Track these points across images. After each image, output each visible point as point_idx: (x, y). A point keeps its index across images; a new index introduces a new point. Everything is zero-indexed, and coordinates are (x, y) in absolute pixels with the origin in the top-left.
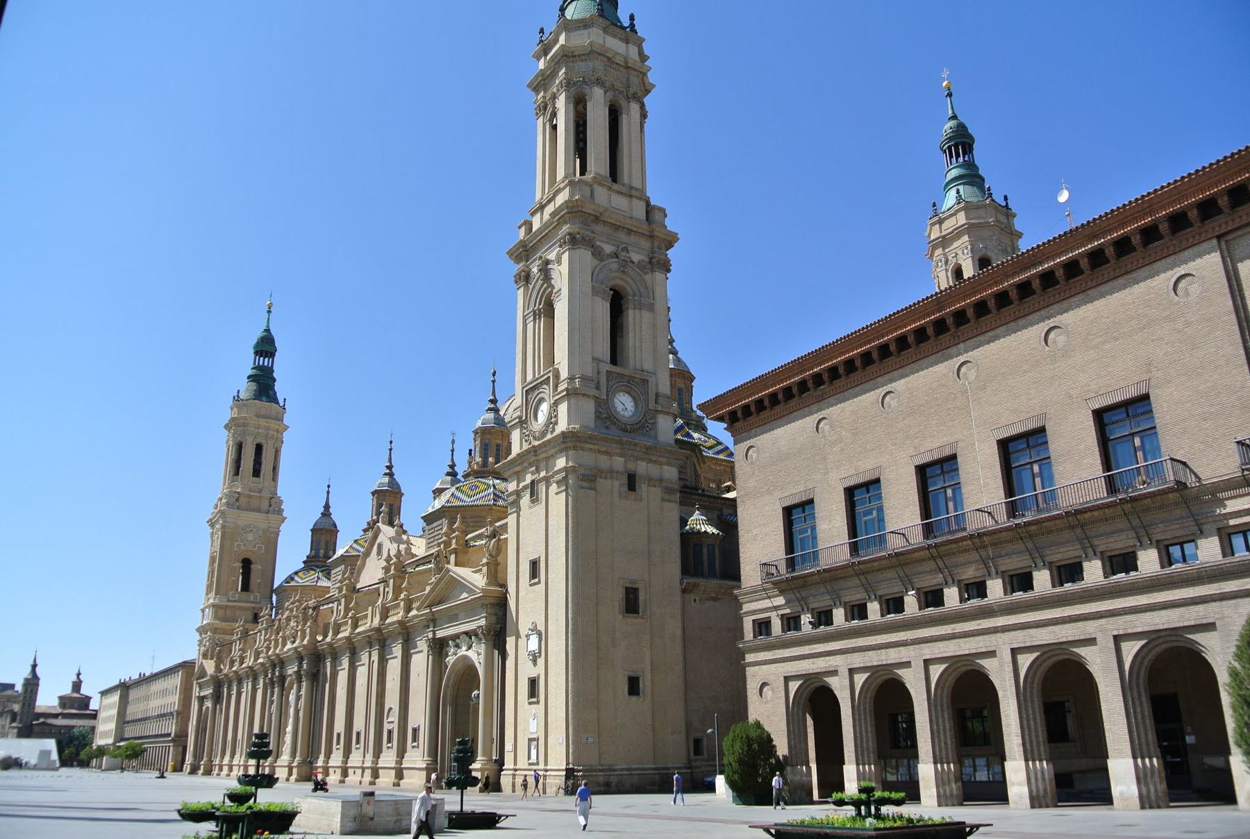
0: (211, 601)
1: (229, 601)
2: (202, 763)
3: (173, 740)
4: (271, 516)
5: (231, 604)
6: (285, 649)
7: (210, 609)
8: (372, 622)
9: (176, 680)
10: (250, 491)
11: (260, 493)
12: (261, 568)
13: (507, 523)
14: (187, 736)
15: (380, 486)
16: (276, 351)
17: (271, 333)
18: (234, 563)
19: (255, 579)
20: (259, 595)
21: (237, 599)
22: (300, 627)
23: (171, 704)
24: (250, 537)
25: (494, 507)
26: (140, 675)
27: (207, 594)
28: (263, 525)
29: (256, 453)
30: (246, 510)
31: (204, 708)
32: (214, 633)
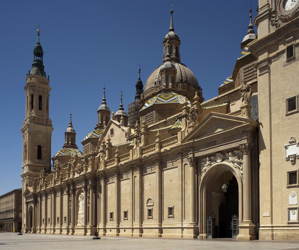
0: (27, 163)
1: (34, 163)
2: (32, 228)
3: (14, 220)
5: (35, 164)
6: (75, 176)
7: (26, 167)
8: (133, 157)
9: (13, 197)
13: (256, 82)
14: (22, 219)
15: (102, 108)
19: (44, 154)
22: (84, 165)
23: (11, 206)
24: (40, 136)
25: (179, 105)
27: (24, 161)
30: (38, 124)
31: (29, 207)
32: (29, 176)
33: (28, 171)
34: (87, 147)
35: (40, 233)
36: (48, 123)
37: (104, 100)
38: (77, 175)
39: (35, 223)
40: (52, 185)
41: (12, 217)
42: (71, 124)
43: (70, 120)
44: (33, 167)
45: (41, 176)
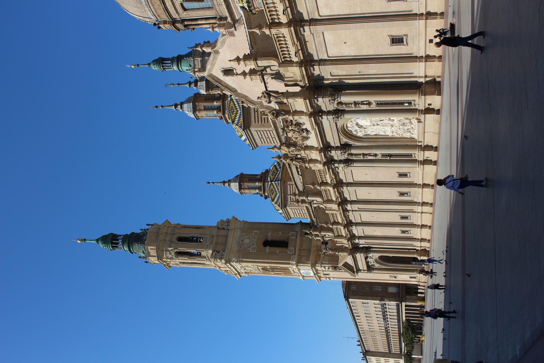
0: (295, 267)
1: (295, 254)
2: (419, 258)
4: (232, 226)
5: (297, 252)
6: (316, 145)
9: (357, 303)
10: (212, 244)
11: (213, 237)
12: (270, 232)
15: (189, 110)
16: (112, 234)
17: (99, 238)
18: (266, 252)
19: (279, 236)
20: (291, 233)
21: (293, 248)
26: (358, 345)
27: (291, 274)
28: (238, 233)
29: (184, 242)
30: (226, 245)
31: (377, 265)
33: (310, 265)
34: (261, 136)
35: (429, 241)
36: (224, 226)
37: (176, 106)
38: (313, 141)
39: (409, 251)
40: (333, 208)
41: (395, 307)
42: (224, 182)
43: (218, 184)
44: (303, 256)
45: (317, 236)
